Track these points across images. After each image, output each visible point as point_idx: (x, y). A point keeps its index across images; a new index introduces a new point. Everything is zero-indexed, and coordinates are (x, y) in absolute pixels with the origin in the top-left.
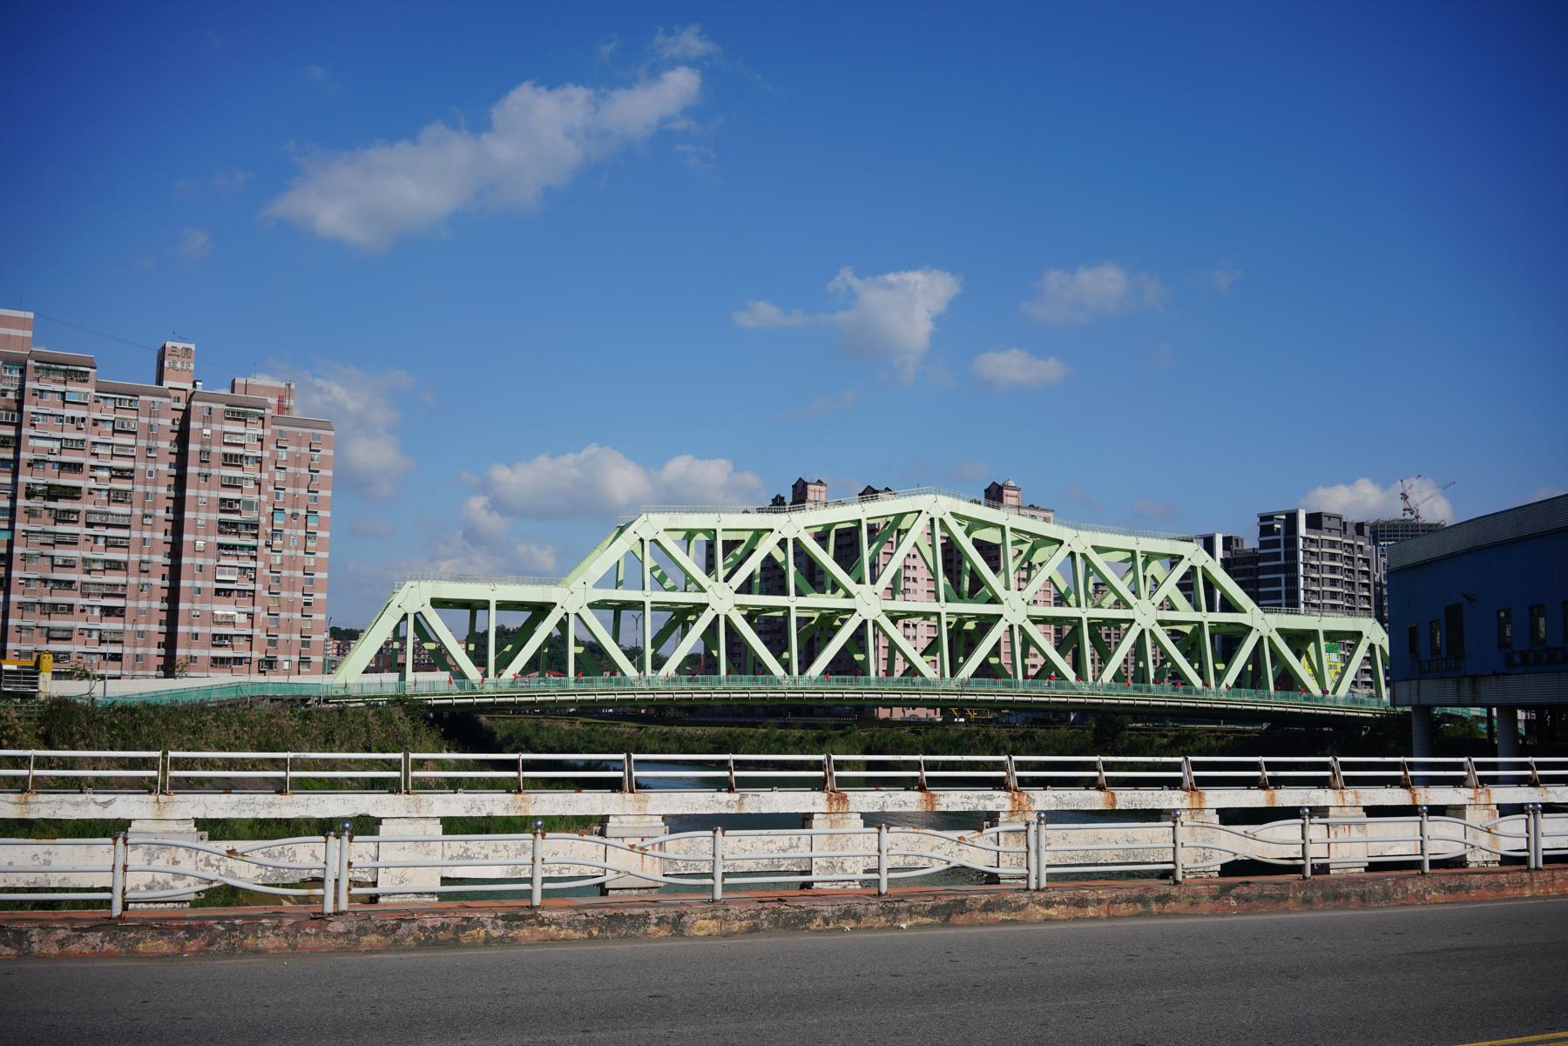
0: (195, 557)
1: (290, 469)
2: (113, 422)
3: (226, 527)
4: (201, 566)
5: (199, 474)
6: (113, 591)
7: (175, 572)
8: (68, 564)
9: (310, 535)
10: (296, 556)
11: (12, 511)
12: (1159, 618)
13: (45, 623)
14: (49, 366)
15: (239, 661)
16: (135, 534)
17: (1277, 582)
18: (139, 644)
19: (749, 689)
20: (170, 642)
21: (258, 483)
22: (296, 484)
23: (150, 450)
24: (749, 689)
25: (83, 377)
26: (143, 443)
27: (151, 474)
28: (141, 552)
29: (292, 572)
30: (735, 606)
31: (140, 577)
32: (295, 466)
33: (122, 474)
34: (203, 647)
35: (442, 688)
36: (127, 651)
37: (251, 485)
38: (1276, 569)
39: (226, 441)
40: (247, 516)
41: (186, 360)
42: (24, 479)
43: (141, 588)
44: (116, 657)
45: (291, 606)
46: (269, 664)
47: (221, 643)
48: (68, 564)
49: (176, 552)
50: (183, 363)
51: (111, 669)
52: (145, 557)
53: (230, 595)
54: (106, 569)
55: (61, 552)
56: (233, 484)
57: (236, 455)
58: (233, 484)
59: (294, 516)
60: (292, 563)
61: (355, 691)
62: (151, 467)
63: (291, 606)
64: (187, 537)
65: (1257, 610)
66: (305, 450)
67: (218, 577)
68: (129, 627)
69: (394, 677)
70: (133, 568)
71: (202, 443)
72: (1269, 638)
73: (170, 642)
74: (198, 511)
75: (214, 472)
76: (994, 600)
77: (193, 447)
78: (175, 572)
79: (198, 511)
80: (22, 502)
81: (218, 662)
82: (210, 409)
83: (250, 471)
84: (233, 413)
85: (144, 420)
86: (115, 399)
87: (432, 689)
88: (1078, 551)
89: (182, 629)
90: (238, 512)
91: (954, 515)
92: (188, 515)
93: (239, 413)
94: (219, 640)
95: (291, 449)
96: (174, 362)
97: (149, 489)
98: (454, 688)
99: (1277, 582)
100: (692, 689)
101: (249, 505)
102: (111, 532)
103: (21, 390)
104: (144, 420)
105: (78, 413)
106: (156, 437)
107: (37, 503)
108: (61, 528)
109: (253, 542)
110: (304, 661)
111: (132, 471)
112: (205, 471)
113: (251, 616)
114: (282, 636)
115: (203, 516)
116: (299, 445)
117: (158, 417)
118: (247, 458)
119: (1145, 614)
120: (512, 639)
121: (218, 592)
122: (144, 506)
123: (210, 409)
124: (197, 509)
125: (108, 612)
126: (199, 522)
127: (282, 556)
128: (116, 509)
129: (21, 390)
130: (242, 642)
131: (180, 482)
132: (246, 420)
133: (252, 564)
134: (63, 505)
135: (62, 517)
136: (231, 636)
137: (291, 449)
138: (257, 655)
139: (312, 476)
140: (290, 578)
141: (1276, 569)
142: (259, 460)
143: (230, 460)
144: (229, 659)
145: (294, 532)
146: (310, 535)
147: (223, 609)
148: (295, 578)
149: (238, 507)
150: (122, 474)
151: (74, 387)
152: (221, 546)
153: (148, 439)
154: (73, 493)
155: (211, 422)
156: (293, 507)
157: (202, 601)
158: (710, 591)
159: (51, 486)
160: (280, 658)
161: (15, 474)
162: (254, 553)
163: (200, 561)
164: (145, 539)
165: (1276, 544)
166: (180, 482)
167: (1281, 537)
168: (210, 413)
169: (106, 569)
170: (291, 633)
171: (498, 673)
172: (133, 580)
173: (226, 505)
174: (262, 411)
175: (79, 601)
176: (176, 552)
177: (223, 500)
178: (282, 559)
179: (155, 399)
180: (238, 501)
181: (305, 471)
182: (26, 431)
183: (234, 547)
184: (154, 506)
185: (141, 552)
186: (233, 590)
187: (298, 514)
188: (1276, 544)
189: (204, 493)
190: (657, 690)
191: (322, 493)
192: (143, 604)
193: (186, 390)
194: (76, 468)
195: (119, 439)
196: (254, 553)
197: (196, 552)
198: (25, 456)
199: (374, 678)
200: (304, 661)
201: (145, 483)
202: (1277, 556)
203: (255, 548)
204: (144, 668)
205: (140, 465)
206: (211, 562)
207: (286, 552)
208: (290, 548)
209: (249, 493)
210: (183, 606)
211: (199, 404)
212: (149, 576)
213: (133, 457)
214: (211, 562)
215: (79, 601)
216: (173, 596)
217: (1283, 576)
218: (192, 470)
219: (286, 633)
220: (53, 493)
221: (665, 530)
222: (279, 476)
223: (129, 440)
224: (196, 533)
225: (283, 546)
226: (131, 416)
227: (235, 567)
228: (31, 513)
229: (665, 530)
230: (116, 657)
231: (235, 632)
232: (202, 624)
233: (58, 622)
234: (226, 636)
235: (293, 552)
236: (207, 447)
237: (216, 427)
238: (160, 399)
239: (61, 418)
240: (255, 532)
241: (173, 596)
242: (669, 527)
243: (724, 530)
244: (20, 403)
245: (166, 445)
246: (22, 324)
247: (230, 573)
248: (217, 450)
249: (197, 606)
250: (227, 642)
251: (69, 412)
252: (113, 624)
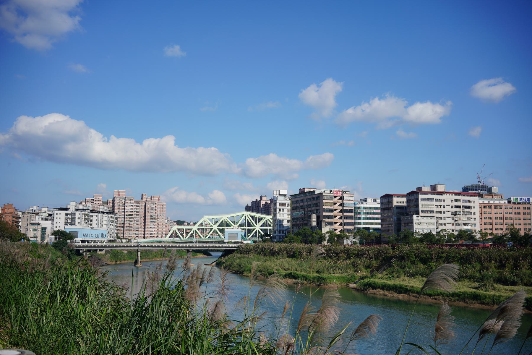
3: (151, 218)
7: (145, 225)
8: (131, 225)
9: (163, 218)
11: (124, 218)
13: (129, 232)
14: (128, 198)
15: (153, 236)
16: (140, 220)
20: (144, 234)
22: (161, 211)
25: (132, 200)
26: (140, 208)
33: (138, 212)
35: (178, 240)
37: (154, 213)
42: (126, 214)
43: (141, 227)
44: (137, 236)
45: (160, 228)
46: (158, 236)
48: (131, 225)
49: (145, 222)
51: (137, 238)
55: (131, 223)
56: (152, 213)
58: (152, 213)
59: (160, 216)
60: (160, 222)
61: (167, 240)
64: (146, 220)
66: (162, 206)
69: (172, 239)
70: (140, 224)
73: (144, 234)
77: (147, 208)
78: (145, 225)
80: (125, 217)
81: (151, 237)
83: (154, 211)
85: (140, 205)
89: (146, 232)
92: (146, 217)
94: (151, 234)
98: (180, 240)
101: (154, 215)
103: (125, 202)
104: (140, 205)
105: (132, 204)
107: (127, 217)
108: (130, 220)
110: (162, 236)
113: (155, 230)
114: (159, 233)
115: (148, 217)
120: (187, 233)
125: (137, 230)
128: (137, 217)
129: (125, 202)
130: (154, 234)
131: (145, 212)
134: (131, 217)
135: (130, 218)
138: (156, 235)
142: (155, 209)
143: (152, 209)
146: (163, 218)
147: (151, 229)
150: (138, 212)
151: (131, 201)
154: (132, 215)
159: (129, 214)
161: (124, 213)
166: (145, 212)
171: (185, 238)
173: (151, 216)
175: (133, 229)
176: (145, 222)
181: (162, 209)
182: (126, 207)
191: (164, 212)
192: (141, 229)
194: (132, 212)
195: (137, 208)
198: (126, 211)
199: (170, 239)
200: (162, 236)
205: (140, 211)
206: (150, 223)
209: (154, 214)
210: (146, 229)
214: (150, 223)
215: (133, 229)
216: (145, 228)
218: (147, 211)
220: (129, 215)
222: (158, 210)
223: (139, 208)
226: (139, 204)
228: (127, 218)
230: (137, 236)
233: (130, 232)
239: (130, 205)
241: (145, 228)
244: (125, 204)
245: (143, 208)
246: (124, 192)
248: (150, 208)
251: (131, 204)
252: (137, 232)
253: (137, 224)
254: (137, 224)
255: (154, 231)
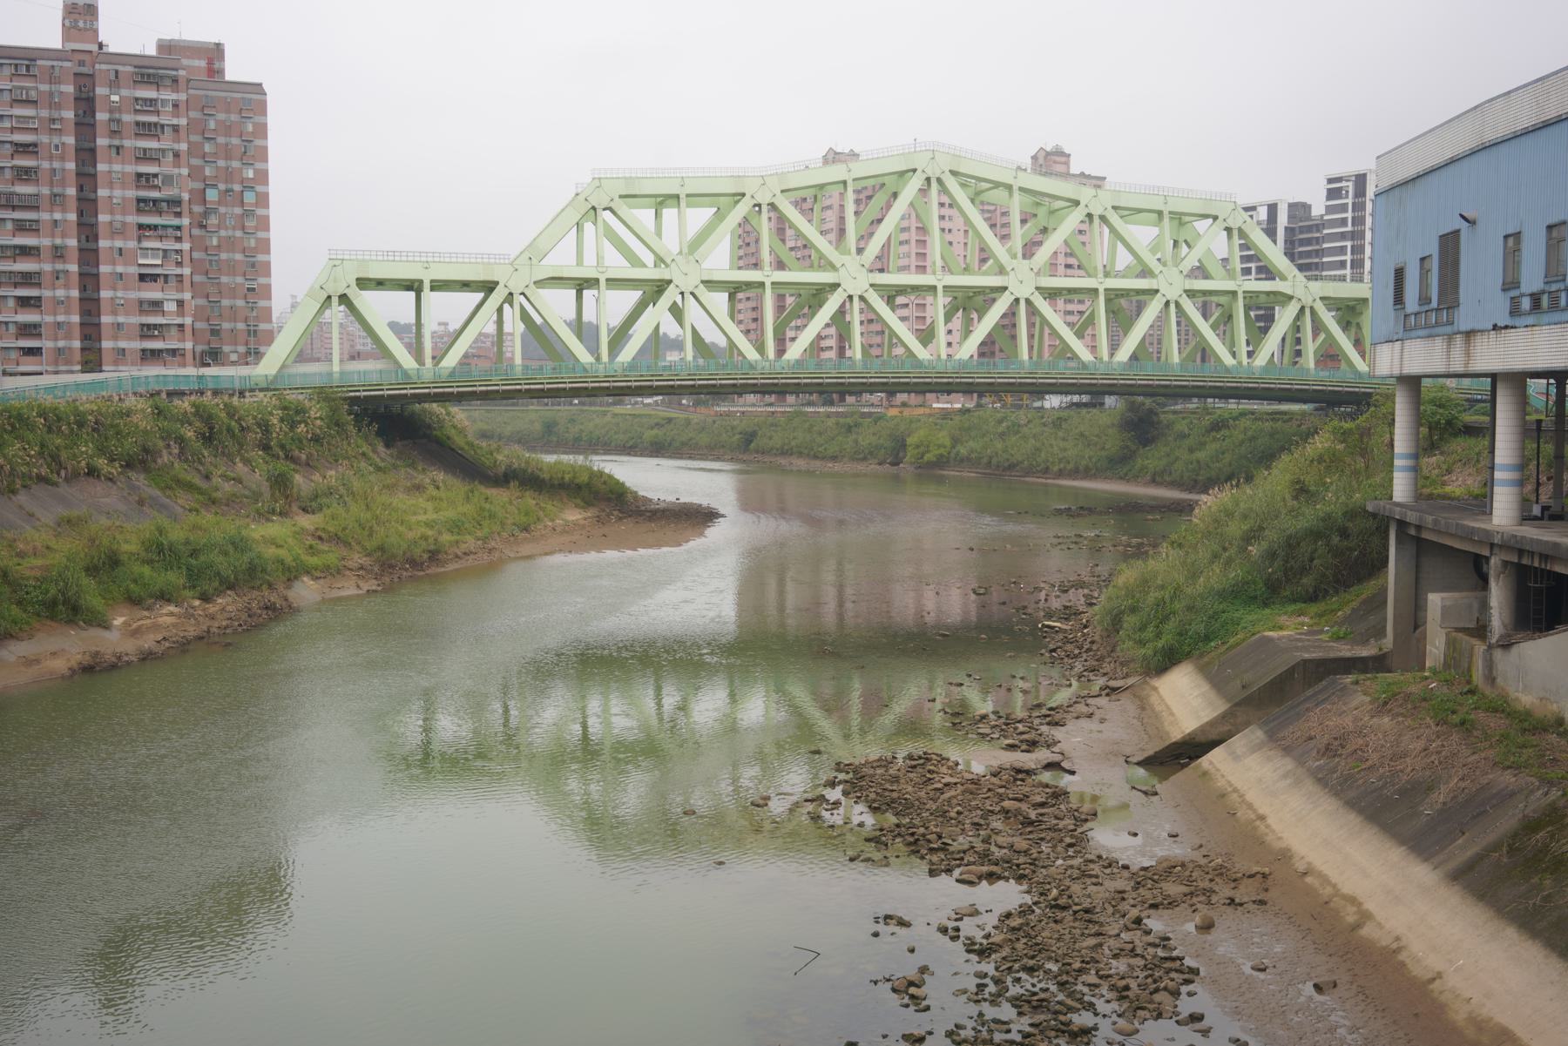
0: (113, 239)
1: (221, 140)
2: (11, 90)
3: (142, 205)
4: (120, 249)
5: (110, 146)
6: (28, 279)
10: (234, 237)
12: (1187, 288)
15: (174, 352)
16: (45, 216)
17: (1342, 250)
18: (59, 336)
19: (717, 374)
21: (177, 155)
23: (53, 121)
24: (717, 374)
27: (57, 147)
28: (53, 236)
29: (231, 255)
30: (703, 282)
31: (53, 263)
32: (226, 136)
34: (130, 339)
36: (46, 344)
38: (1343, 236)
39: (138, 107)
40: (167, 193)
41: (88, 18)
43: (57, 275)
45: (233, 293)
47: (149, 333)
50: (85, 22)
52: (58, 241)
53: (156, 281)
54: (15, 255)
56: (145, 156)
57: (150, 124)
58: (145, 156)
60: (229, 243)
62: (56, 140)
63: (233, 293)
65: (1300, 276)
67: (140, 262)
68: (49, 319)
71: (111, 111)
72: (1312, 308)
74: (111, 188)
75: (127, 143)
76: (1002, 271)
79: (111, 188)
82: (117, 72)
83: (165, 143)
84: (143, 75)
86: (11, 64)
87: (362, 379)
88: (1096, 212)
90: (156, 187)
91: (954, 173)
93: (149, 75)
94: (147, 331)
95: (221, 116)
96: (76, 21)
97: (56, 165)
99: (1342, 250)
100: (652, 376)
101: (168, 180)
102: (18, 215)
104: (44, 87)
106: (59, 106)
109: (175, 222)
111: (35, 145)
112: (116, 142)
113: (180, 303)
114: (226, 326)
115: (117, 193)
116: (228, 111)
117: (59, 83)
118: (163, 126)
119: (1171, 284)
121: (142, 277)
122: (51, 184)
123: (117, 72)
124: (111, 185)
125: (24, 302)
126: (115, 201)
127: (219, 237)
132: (157, 83)
133: (177, 246)
136: (161, 325)
137: (221, 116)
139: (245, 146)
140: (227, 260)
141: (1343, 236)
142: (176, 128)
144: (160, 351)
145: (230, 210)
147: (152, 293)
148: (234, 261)
149: (156, 183)
152: (141, 227)
153: (50, 108)
155: (119, 87)
156: (226, 182)
157: (125, 289)
158: (673, 265)
160: (226, 349)
162: (179, 234)
163: (118, 244)
164: (56, 221)
165: (1343, 208)
167: (1350, 201)
168: (117, 77)
169: (15, 255)
170: (235, 322)
172: (47, 267)
174: (174, 73)
177: (139, 175)
178: (219, 241)
179: (55, 63)
180: (155, 176)
183: (155, 227)
184: (63, 183)
185: (53, 236)
186: (158, 275)
187: (232, 191)
188: (1343, 208)
189: (117, 167)
190: (613, 376)
192: (60, 293)
193: (91, 52)
196: (179, 234)
197: (116, 232)
201: (51, 158)
202: (1344, 222)
203: (179, 228)
204: (68, 362)
205: (44, 139)
207: (223, 233)
208: (227, 229)
209: (166, 168)
211: (104, 67)
212: (64, 262)
213: (36, 129)
217: (1349, 244)
219: (230, 321)
221: (621, 197)
223: (28, 112)
224: (112, 213)
225: (219, 226)
227: (158, 249)
229: (621, 197)
231: (164, 322)
232: (127, 314)
234: (155, 326)
235: (230, 233)
236: (117, 116)
237: (125, 92)
238: (60, 63)
240: (179, 210)
242: (624, 193)
243: (688, 196)
247: (154, 257)
248: (128, 118)
249: (120, 294)
250: (156, 333)
253: (25, 252)
254: (25, 252)
255: (170, 307)
